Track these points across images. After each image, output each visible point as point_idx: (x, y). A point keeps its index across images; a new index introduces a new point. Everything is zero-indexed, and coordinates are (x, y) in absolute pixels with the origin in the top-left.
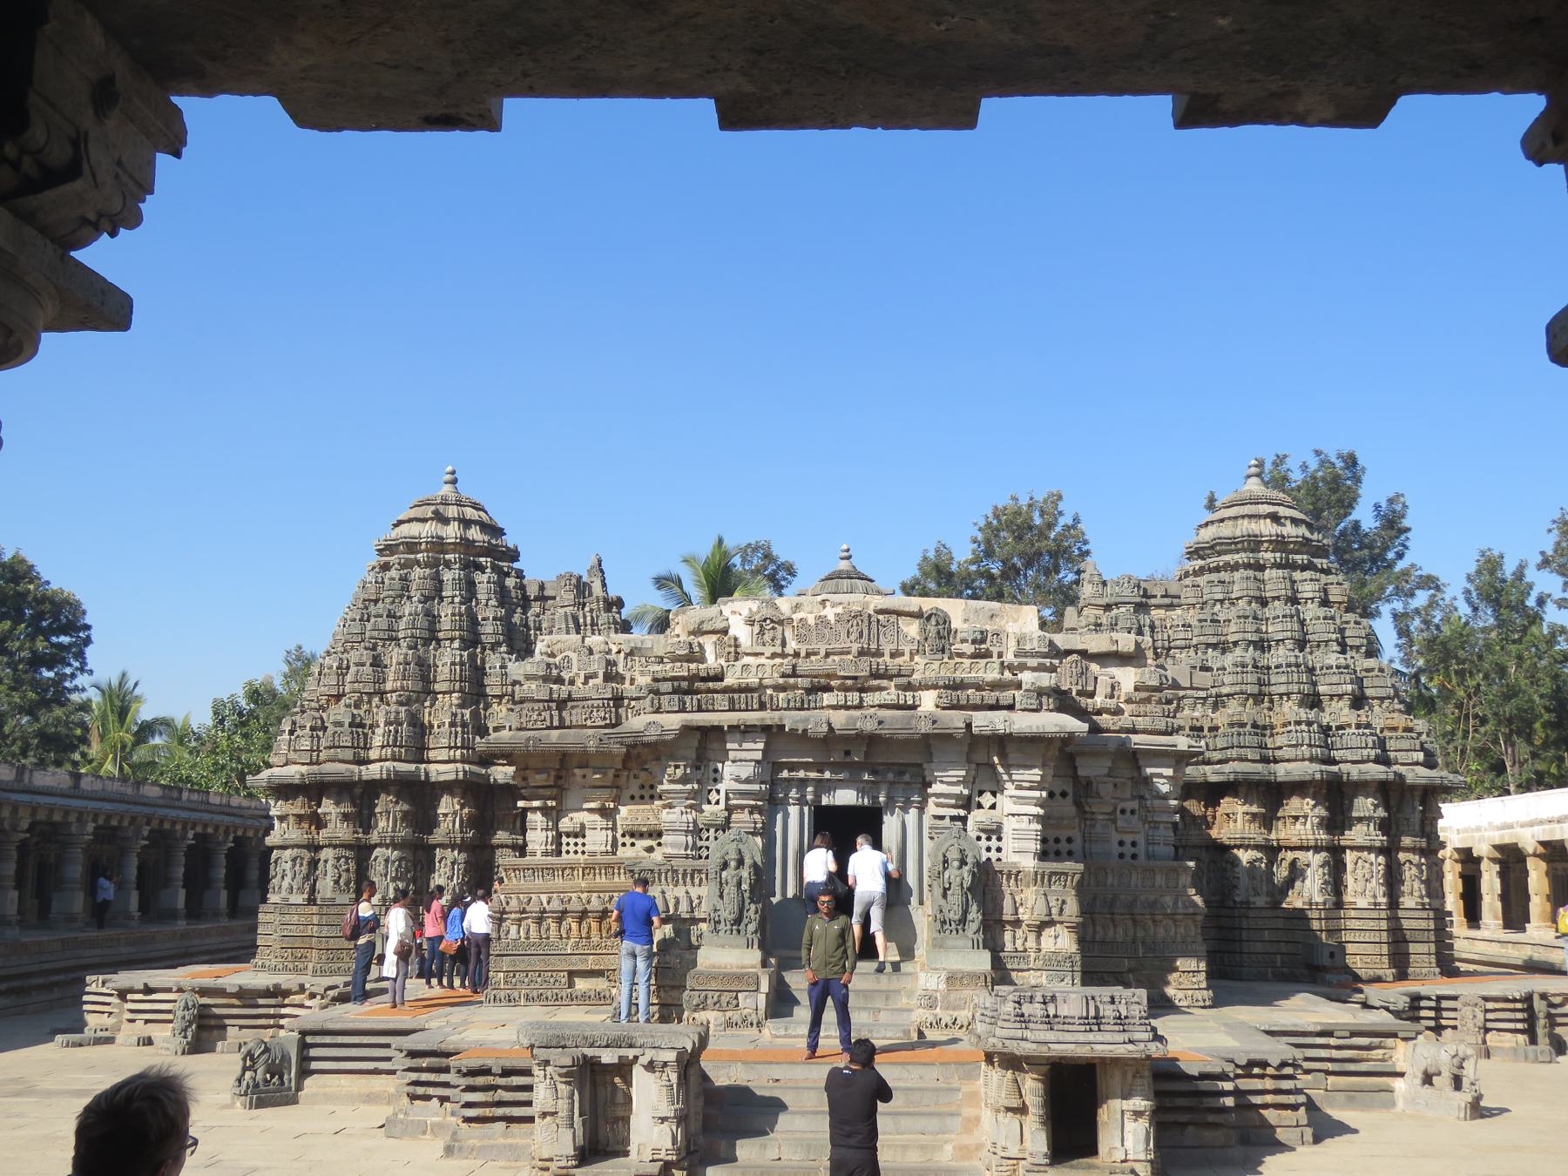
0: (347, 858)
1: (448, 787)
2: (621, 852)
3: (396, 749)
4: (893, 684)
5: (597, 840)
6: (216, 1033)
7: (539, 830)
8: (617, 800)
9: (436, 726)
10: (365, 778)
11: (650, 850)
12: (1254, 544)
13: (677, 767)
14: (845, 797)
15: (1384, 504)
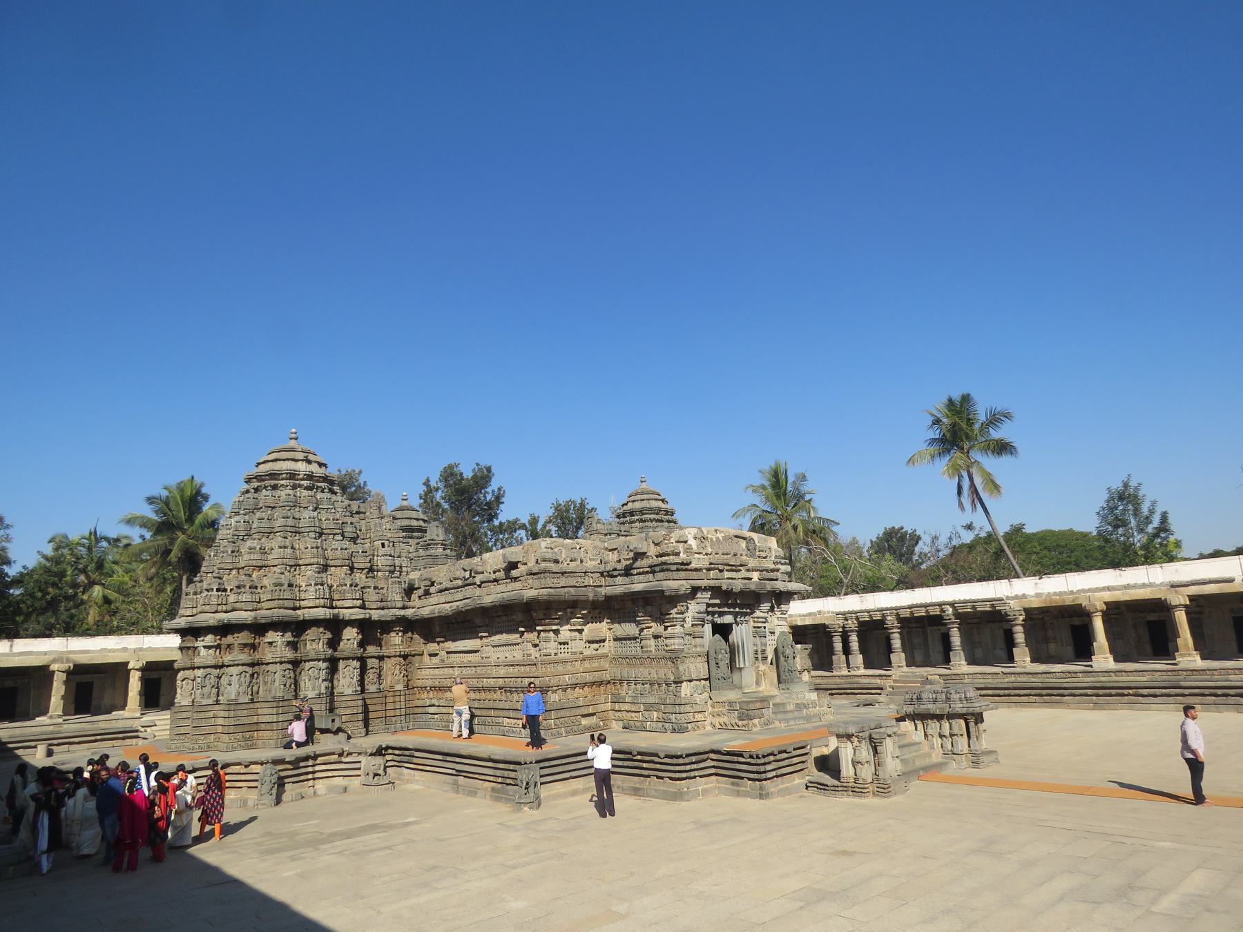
0: (290, 669)
1: (351, 623)
2: (584, 651)
3: (326, 600)
4: (741, 568)
5: (578, 645)
6: (280, 789)
7: (552, 641)
8: (584, 624)
9: (335, 586)
10: (307, 618)
11: (597, 650)
12: (658, 511)
13: (683, 606)
14: (728, 619)
15: (496, 491)
